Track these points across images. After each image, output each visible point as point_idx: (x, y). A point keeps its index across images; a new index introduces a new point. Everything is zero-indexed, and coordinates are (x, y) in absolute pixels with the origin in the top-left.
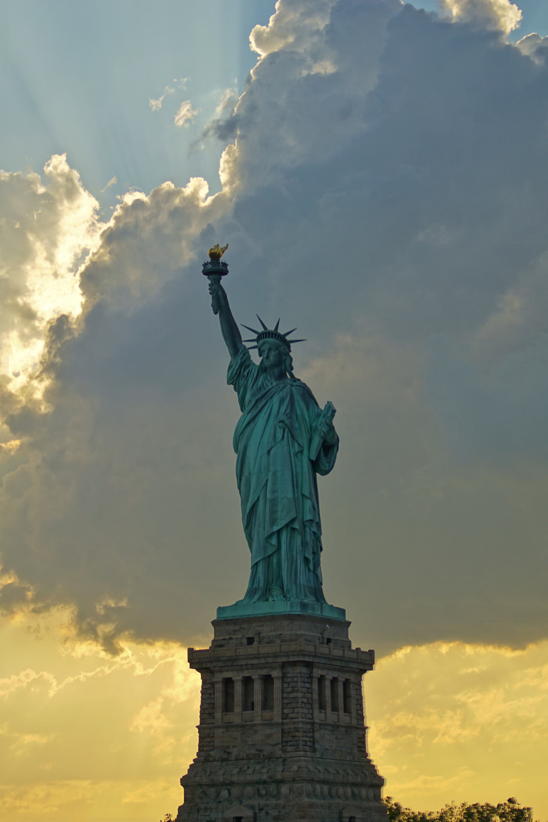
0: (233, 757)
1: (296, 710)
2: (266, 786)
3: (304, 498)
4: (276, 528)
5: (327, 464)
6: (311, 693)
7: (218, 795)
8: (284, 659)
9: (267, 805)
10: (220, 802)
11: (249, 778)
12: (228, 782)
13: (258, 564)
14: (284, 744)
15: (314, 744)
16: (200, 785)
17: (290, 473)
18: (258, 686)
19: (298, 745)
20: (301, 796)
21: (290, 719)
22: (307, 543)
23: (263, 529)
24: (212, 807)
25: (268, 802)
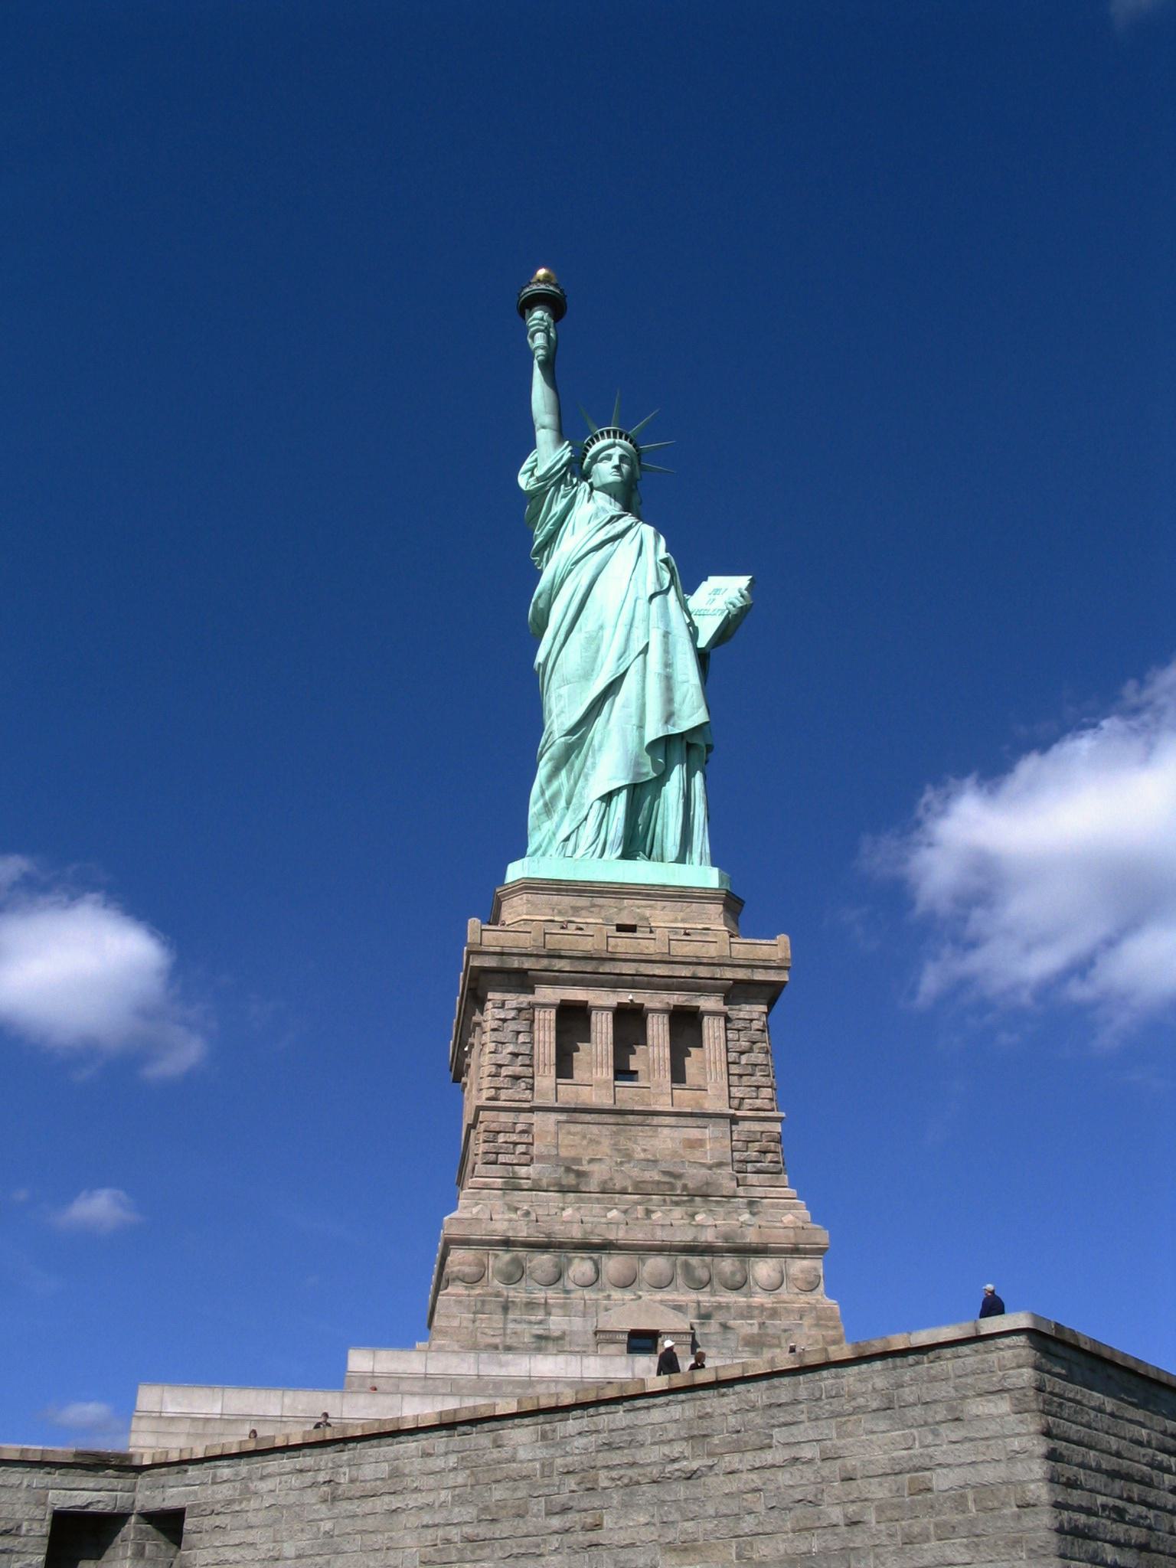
0: (593, 1184)
1: (766, 1092)
2: (708, 1259)
7: (559, 1277)
8: (741, 974)
9: (719, 1307)
11: (661, 1236)
12: (596, 1240)
13: (617, 792)
14: (737, 1166)
16: (507, 1243)
18: (658, 1028)
20: (811, 1291)
21: (750, 1110)
23: (635, 727)
24: (549, 1301)
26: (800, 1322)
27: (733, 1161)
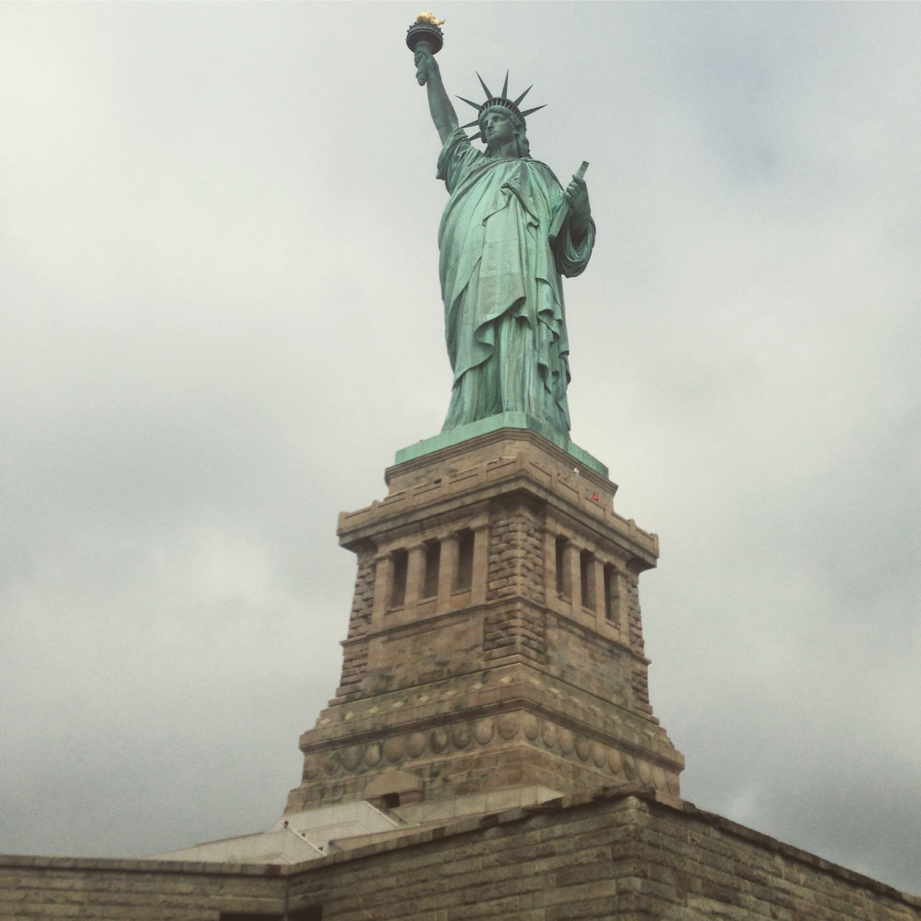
0: (395, 685)
1: (511, 580)
2: (448, 727)
3: (539, 283)
4: (490, 317)
5: (578, 257)
6: (543, 558)
8: (492, 493)
9: (446, 764)
10: (363, 772)
11: (418, 714)
12: (379, 728)
14: (488, 644)
15: (546, 649)
16: (332, 744)
17: (517, 243)
19: (512, 643)
20: (512, 738)
22: (541, 345)
25: (449, 758)
26: (493, 767)
27: (485, 640)
